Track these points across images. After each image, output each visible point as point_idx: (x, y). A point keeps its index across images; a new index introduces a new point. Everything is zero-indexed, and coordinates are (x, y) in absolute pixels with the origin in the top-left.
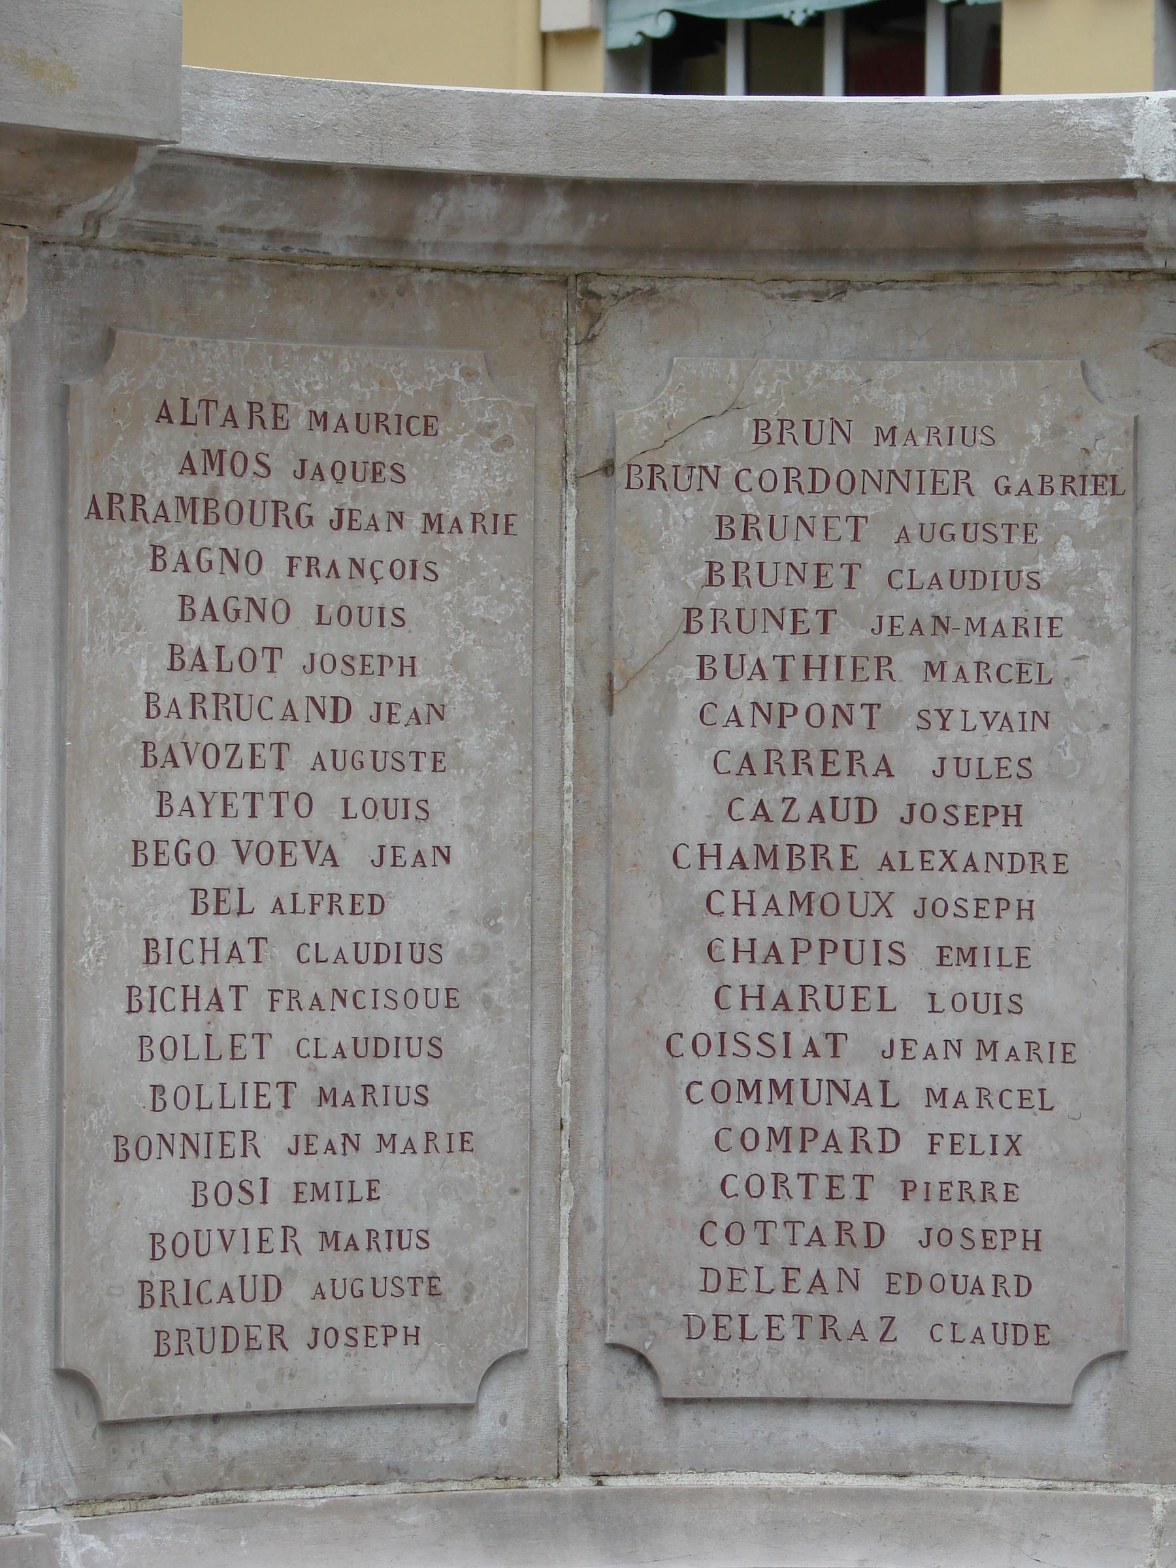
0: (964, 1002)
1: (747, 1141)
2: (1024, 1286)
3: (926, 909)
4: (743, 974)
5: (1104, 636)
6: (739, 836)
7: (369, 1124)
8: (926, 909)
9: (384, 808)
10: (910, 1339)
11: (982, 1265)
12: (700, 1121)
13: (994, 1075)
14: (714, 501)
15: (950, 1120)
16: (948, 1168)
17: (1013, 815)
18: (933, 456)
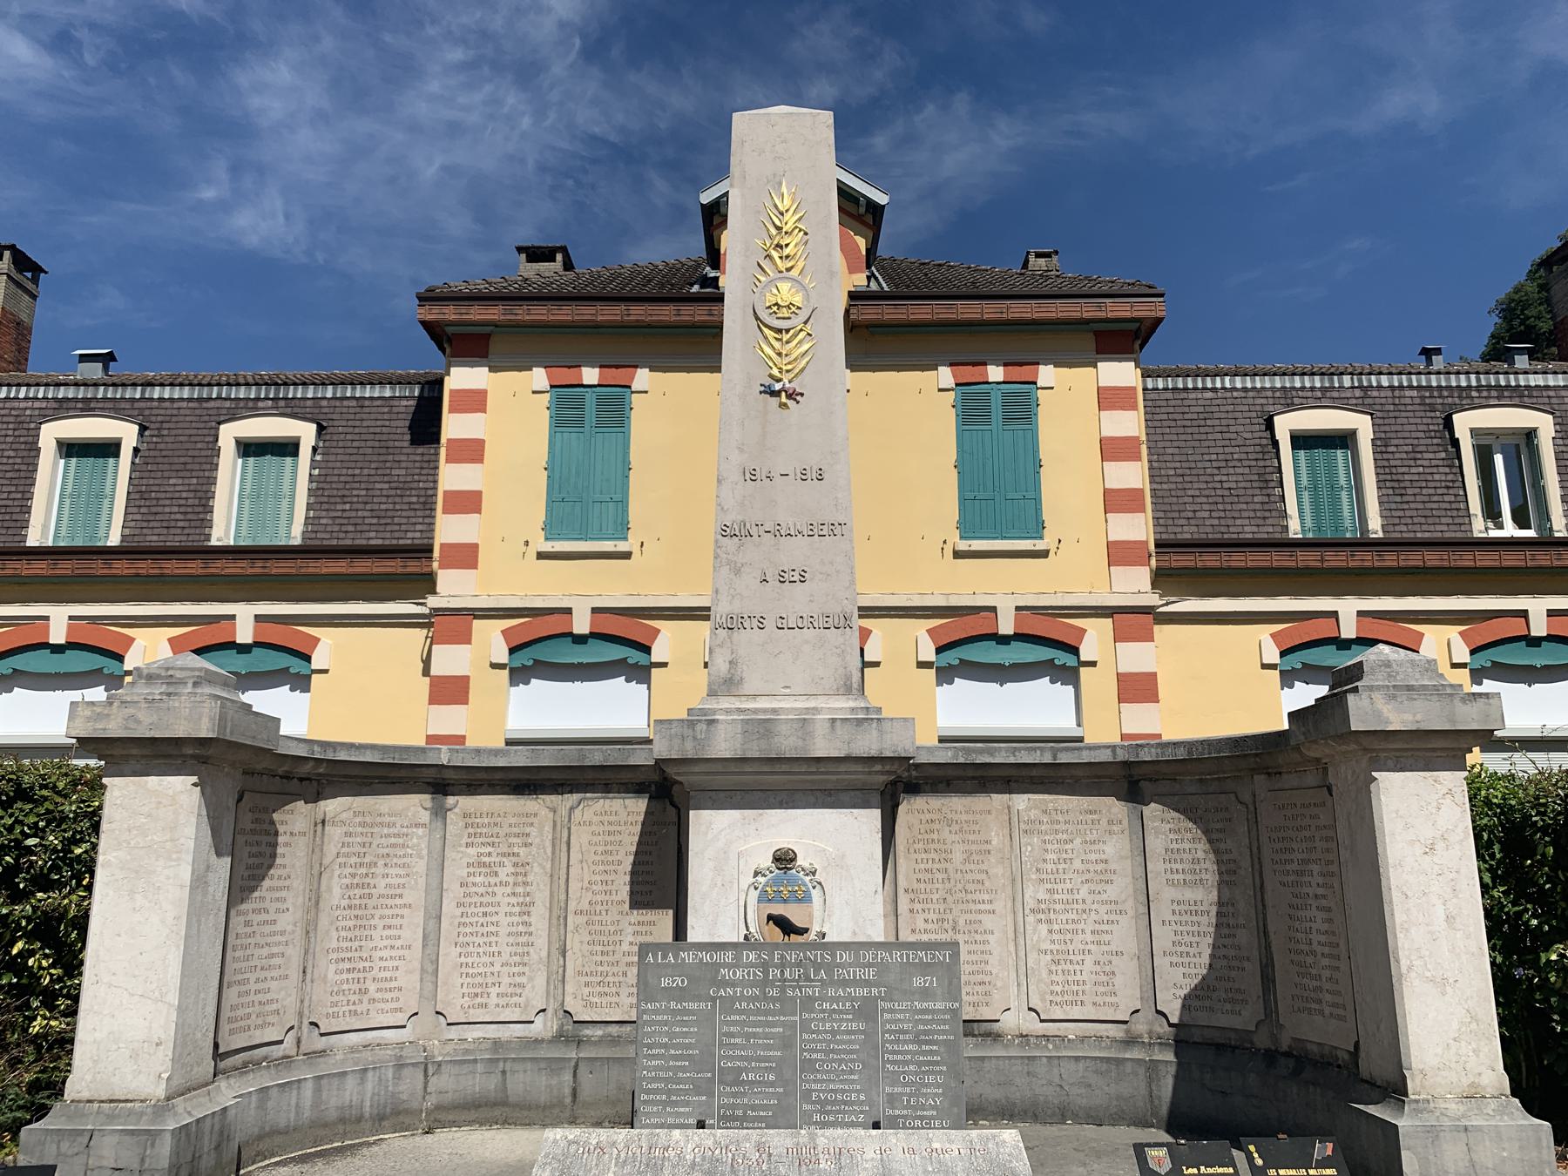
0: (388, 937)
2: (398, 999)
3: (382, 917)
4: (343, 934)
5: (421, 858)
6: (345, 903)
7: (268, 974)
8: (382, 917)
10: (373, 1014)
11: (388, 996)
12: (333, 967)
13: (394, 953)
14: (345, 829)
16: (383, 974)
17: (401, 896)
18: (387, 819)
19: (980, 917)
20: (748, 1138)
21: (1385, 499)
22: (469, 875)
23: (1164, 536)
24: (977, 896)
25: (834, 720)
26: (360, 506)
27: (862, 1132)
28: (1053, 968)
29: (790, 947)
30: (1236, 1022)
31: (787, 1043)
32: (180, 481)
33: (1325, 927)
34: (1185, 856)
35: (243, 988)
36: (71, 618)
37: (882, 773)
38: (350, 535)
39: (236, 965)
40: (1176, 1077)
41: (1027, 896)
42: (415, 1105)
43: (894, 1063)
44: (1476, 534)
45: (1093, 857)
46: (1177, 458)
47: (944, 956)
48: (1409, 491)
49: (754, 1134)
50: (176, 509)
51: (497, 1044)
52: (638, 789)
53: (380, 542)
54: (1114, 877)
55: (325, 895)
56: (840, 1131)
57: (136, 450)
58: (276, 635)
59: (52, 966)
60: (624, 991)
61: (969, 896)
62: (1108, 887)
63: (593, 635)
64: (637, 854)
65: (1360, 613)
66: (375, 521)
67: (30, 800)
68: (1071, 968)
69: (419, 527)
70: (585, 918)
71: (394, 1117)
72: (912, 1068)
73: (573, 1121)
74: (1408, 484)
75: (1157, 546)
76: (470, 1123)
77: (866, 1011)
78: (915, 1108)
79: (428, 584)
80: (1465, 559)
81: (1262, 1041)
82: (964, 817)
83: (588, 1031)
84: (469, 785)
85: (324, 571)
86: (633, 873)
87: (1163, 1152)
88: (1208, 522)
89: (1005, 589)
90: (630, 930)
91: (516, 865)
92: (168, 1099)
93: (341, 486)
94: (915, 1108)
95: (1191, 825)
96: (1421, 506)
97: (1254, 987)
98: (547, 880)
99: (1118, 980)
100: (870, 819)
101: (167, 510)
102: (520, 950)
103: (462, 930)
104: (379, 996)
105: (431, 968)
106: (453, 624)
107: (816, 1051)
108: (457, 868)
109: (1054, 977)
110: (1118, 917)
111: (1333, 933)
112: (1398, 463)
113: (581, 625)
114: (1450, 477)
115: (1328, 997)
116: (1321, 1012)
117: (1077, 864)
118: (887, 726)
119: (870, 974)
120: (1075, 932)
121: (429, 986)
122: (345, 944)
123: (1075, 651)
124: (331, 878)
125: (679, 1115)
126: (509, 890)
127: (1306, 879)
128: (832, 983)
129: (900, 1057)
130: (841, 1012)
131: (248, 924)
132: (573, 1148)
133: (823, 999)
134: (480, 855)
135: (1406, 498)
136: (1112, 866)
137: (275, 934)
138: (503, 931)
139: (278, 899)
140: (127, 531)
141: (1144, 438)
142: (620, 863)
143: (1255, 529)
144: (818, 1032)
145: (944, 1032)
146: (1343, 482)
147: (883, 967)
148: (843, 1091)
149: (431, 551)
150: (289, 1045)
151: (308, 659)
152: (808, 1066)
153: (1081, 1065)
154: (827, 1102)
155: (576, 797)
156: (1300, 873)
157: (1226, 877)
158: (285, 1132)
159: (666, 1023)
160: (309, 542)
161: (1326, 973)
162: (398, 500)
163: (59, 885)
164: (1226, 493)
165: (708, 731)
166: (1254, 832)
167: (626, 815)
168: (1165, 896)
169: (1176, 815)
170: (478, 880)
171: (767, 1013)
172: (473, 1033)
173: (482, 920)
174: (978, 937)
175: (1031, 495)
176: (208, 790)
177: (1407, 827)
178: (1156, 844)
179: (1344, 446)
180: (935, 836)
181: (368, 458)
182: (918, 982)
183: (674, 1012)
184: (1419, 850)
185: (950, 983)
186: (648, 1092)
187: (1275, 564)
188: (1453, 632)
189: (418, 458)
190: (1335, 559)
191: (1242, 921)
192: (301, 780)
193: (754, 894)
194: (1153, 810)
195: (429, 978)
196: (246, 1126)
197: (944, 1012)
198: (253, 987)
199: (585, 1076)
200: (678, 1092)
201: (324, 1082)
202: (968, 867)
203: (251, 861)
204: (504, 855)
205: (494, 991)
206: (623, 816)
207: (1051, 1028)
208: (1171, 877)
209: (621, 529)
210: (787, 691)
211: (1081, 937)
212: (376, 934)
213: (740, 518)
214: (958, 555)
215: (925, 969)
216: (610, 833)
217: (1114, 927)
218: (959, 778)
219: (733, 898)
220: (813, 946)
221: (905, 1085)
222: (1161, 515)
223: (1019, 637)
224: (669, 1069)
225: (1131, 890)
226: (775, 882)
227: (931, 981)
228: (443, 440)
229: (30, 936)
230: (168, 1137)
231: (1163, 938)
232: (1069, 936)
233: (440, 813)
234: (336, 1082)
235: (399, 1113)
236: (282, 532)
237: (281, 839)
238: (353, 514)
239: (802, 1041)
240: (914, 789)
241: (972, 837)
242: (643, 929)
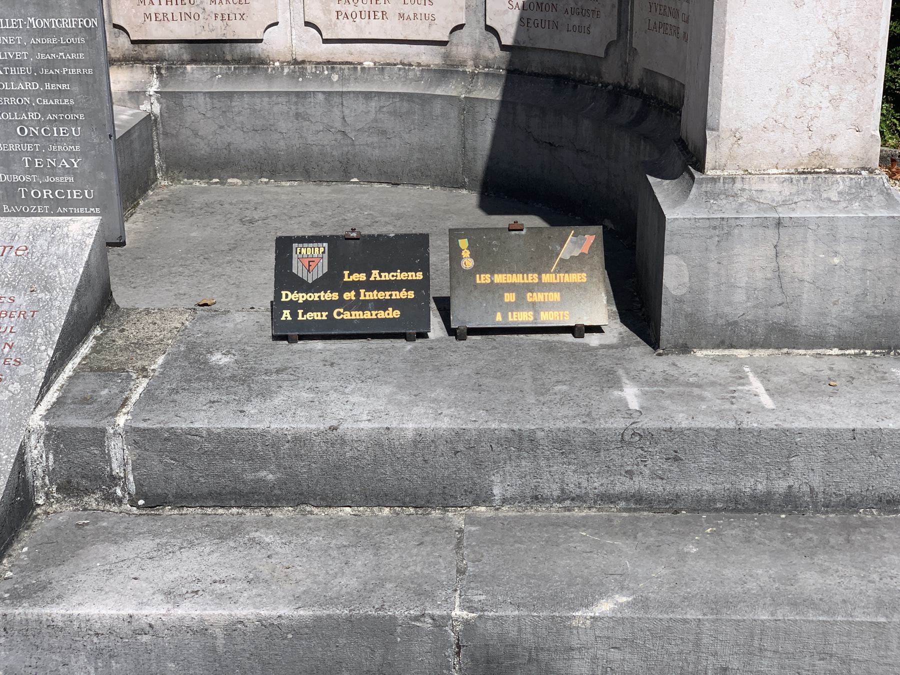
40: (501, 123)
72: (32, 115)
81: (611, 73)
94: (41, 172)
129: (14, 101)
153: (373, 104)
197: (75, 32)
207: (339, 52)
221: (24, 140)
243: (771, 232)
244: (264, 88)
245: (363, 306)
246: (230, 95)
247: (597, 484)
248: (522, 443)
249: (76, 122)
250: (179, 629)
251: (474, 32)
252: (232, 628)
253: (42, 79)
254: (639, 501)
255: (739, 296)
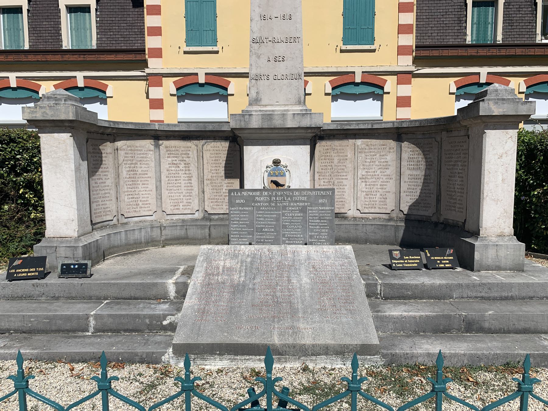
1: (129, 198)
3: (141, 181)
4: (129, 186)
6: (128, 176)
8: (141, 181)
9: (105, 175)
11: (146, 206)
12: (126, 197)
13: (146, 192)
14: (125, 152)
15: (143, 196)
16: (143, 199)
17: (147, 174)
19: (342, 181)
20: (265, 248)
21: (505, 28)
22: (169, 167)
23: (419, 43)
24: (342, 174)
25: (294, 114)
26: (117, 33)
27: (301, 246)
28: (366, 197)
29: (279, 190)
30: (426, 214)
31: (277, 220)
32: (47, 23)
33: (460, 183)
34: (415, 160)
35: (97, 204)
36: (16, 77)
37: (311, 133)
38: (114, 45)
39: (94, 196)
40: (405, 231)
41: (359, 174)
42: (158, 239)
43: (312, 226)
44: (537, 42)
45: (383, 160)
46: (427, 11)
47: (330, 193)
48: (515, 24)
49: (267, 247)
50: (47, 35)
51: (183, 221)
52: (225, 139)
53: (125, 48)
54: (389, 167)
55: (121, 174)
56: (294, 246)
57: (28, 10)
58: (92, 83)
59: (34, 197)
60: (224, 204)
61: (339, 174)
62: (387, 170)
63: (206, 83)
64: (226, 161)
65: (488, 73)
66: (123, 39)
67: (15, 143)
68: (371, 196)
69: (139, 42)
70: (210, 182)
71: (152, 242)
73: (209, 243)
74: (515, 21)
75: (416, 47)
76: (176, 244)
77: (303, 210)
78: (318, 239)
79: (144, 64)
80: (531, 52)
81: (434, 219)
82: (339, 148)
83: (213, 217)
84: (167, 137)
85: (106, 59)
86: (225, 167)
87: (398, 252)
88: (436, 38)
89: (358, 64)
90: (225, 185)
91: (185, 164)
92: (79, 237)
93: (108, 25)
94: (318, 239)
95: (418, 149)
96: (518, 30)
97: (434, 202)
98: (196, 169)
99: (388, 201)
100: (307, 149)
101: (44, 35)
102: (189, 191)
103: (169, 185)
104: (143, 206)
105: (159, 197)
106: (155, 79)
107: (287, 222)
108: (165, 165)
109: (366, 200)
110: (390, 180)
111: (463, 185)
112: (512, 12)
113: (202, 80)
114: (531, 19)
115: (458, 205)
116: (455, 210)
117: (377, 163)
118: (313, 116)
119: (305, 198)
120: (374, 185)
121: (159, 203)
122: (130, 190)
123: (382, 88)
124: (122, 168)
125: (243, 241)
126: (183, 172)
127: (456, 167)
128: (292, 201)
130: (295, 210)
131: (96, 183)
132: (210, 251)
133: (289, 206)
134: (172, 161)
135: (513, 27)
136: (389, 163)
137: (105, 186)
138: (183, 185)
139: (105, 175)
140: (31, 44)
141: (415, 3)
142: (221, 164)
143: (454, 40)
144: (287, 216)
145: (328, 216)
146: (490, 21)
147: (309, 197)
148: (296, 234)
149: (145, 51)
150: (115, 221)
151: (105, 92)
152: (284, 227)
153: (373, 227)
154: (290, 237)
155: (204, 141)
156: (454, 165)
157: (428, 167)
158: (118, 247)
159: (238, 214)
160: (99, 48)
161: (459, 198)
162: (130, 30)
163: (31, 171)
164: (445, 26)
165: (249, 118)
166: (440, 151)
167: (223, 146)
168: (406, 173)
169: (413, 146)
170: (173, 169)
171: (271, 211)
172: (175, 217)
173: (175, 182)
174: (341, 187)
175: (370, 27)
176: (76, 138)
177: (494, 149)
178: (405, 156)
179: (493, 6)
180: (328, 154)
181: (117, 13)
182: (321, 201)
183: (241, 211)
184: (497, 157)
185: (331, 201)
186: (233, 234)
187: (459, 54)
188: (521, 80)
189: (136, 13)
190: (482, 52)
191: (432, 181)
192: (108, 135)
193: (266, 174)
194: (405, 144)
195: (159, 200)
196: (105, 244)
197: (329, 210)
198: (101, 203)
199: (213, 231)
200: (243, 235)
201: (128, 232)
202: (339, 164)
203: (94, 162)
204: (181, 161)
205: (181, 204)
206: (221, 148)
208: (409, 167)
209: (215, 42)
210: (277, 103)
211: (376, 187)
212: (140, 186)
213: (259, 35)
214: (342, 51)
215: (323, 197)
216: (217, 154)
217: (388, 184)
218: (337, 134)
219: (259, 175)
220: (286, 190)
221: (315, 232)
222: (419, 35)
223: (362, 83)
224: (240, 228)
225: (395, 171)
226: (274, 170)
227: (325, 201)
228: (145, 6)
229: (25, 188)
230: (81, 248)
231: (404, 187)
232: (372, 186)
233: (157, 146)
234: (132, 232)
235: (153, 241)
236: (89, 44)
237: (103, 155)
238: (114, 36)
239: (282, 219)
240: (322, 138)
241: (341, 154)
242: (230, 185)
243: (496, 247)
244: (348, 223)
245: (409, 263)
246: (341, 225)
247: (474, 294)
248: (460, 286)
249: (327, 229)
250: (410, 317)
251: (398, 211)
252: (421, 317)
253: (321, 220)
254: (482, 298)
255: (490, 260)
